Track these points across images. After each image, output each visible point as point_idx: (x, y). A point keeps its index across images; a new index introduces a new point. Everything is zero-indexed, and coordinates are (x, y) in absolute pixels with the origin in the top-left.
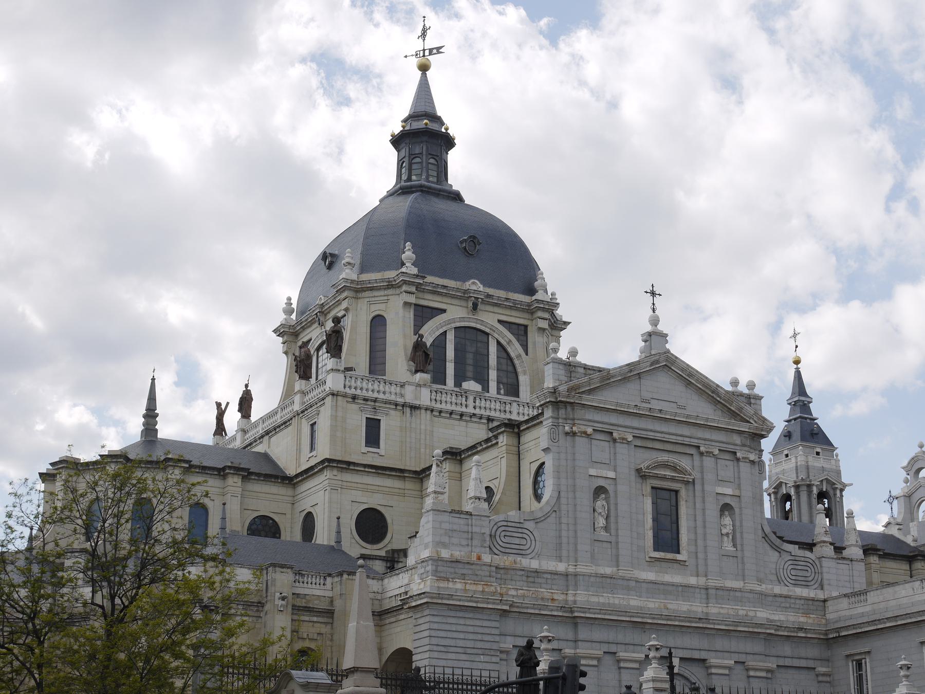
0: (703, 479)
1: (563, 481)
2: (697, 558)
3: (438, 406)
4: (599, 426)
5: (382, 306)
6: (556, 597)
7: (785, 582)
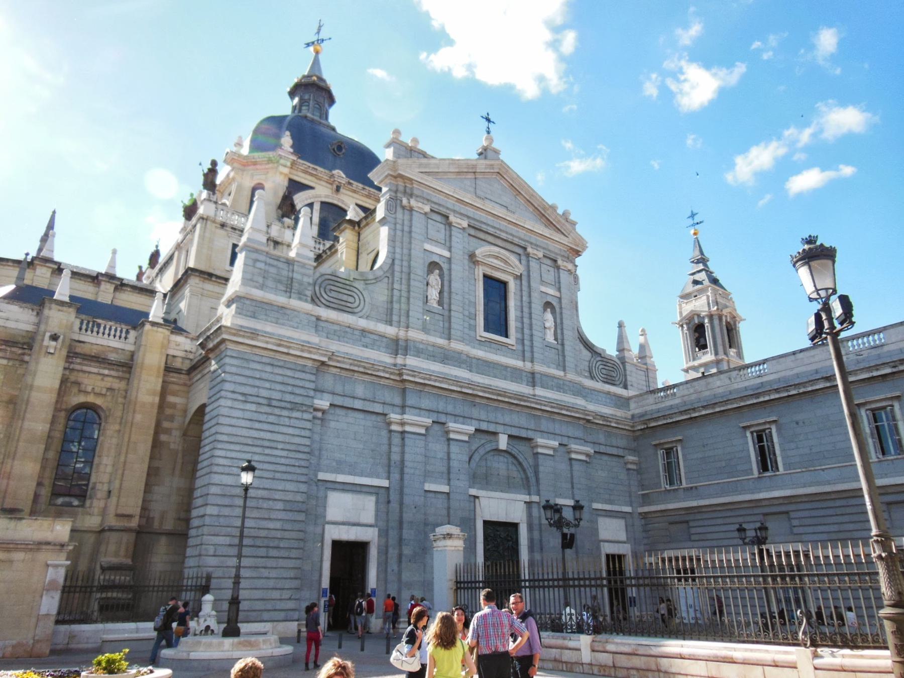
0: (529, 276)
2: (523, 344)
5: (263, 177)
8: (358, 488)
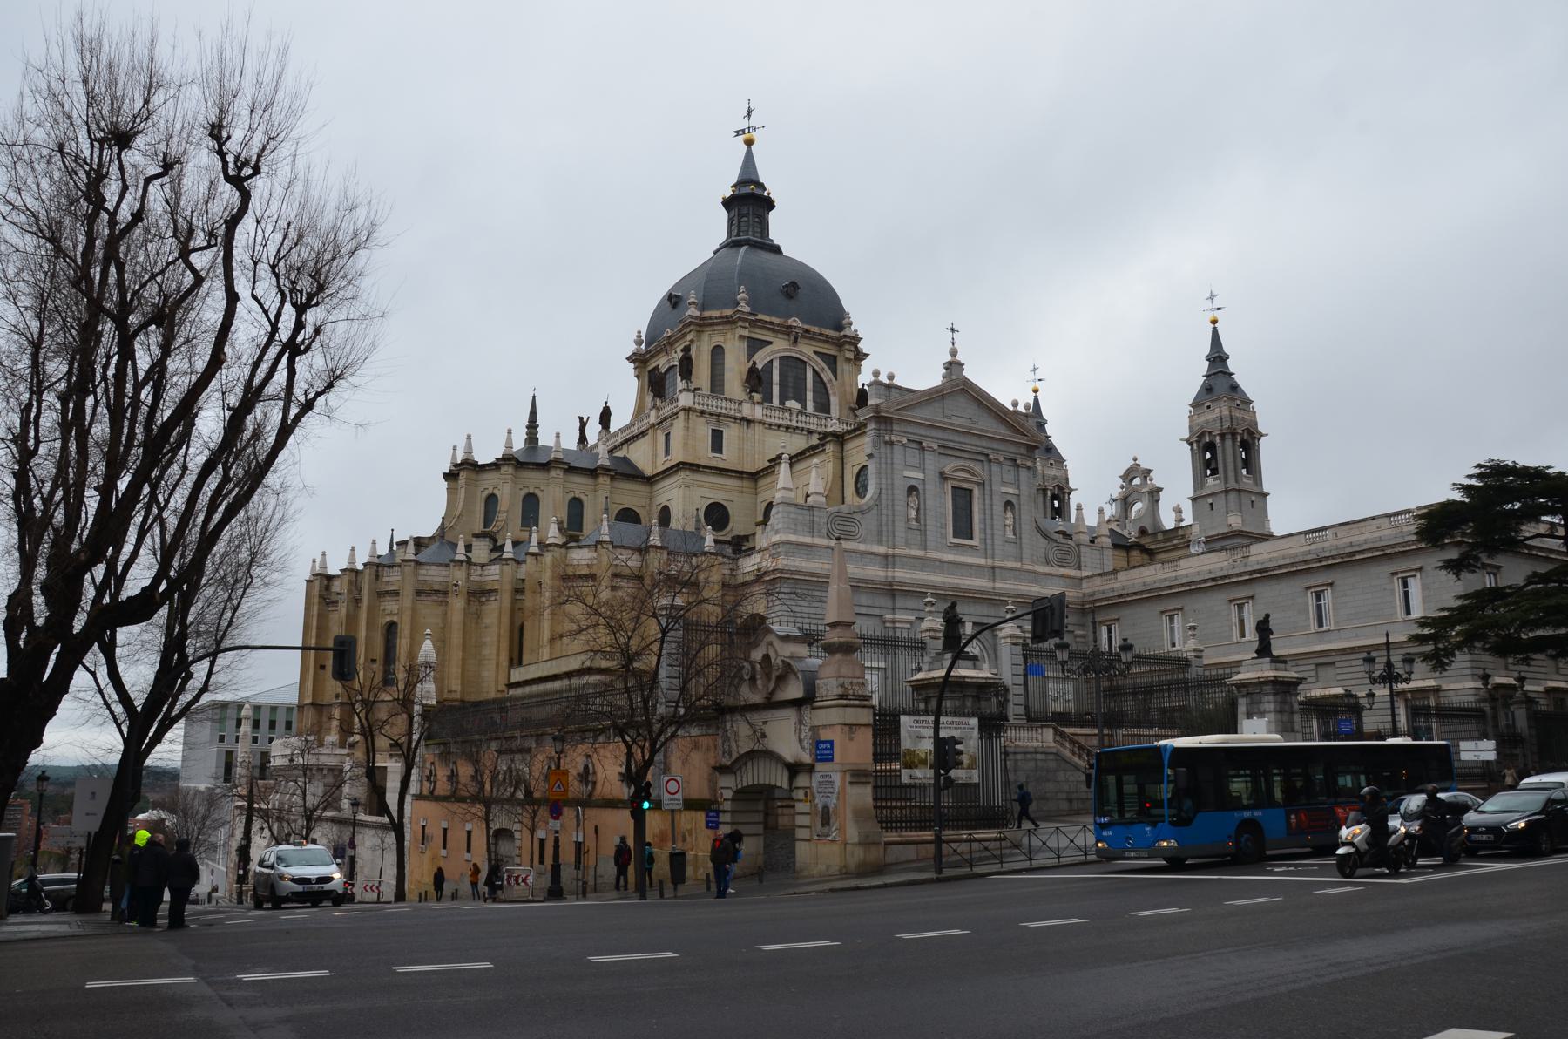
0: (991, 480)
1: (884, 481)
2: (986, 544)
3: (768, 420)
4: (912, 437)
5: (722, 339)
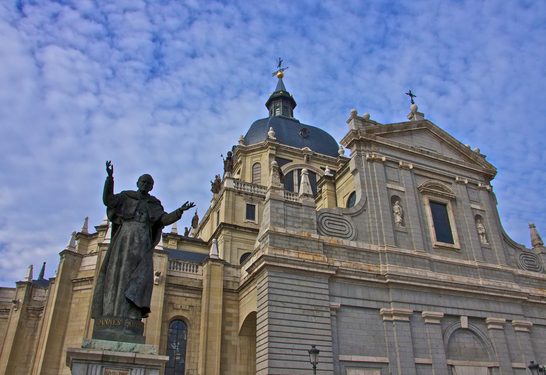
5: (259, 159)
6: (371, 269)
7: (523, 267)
8: (367, 365)
